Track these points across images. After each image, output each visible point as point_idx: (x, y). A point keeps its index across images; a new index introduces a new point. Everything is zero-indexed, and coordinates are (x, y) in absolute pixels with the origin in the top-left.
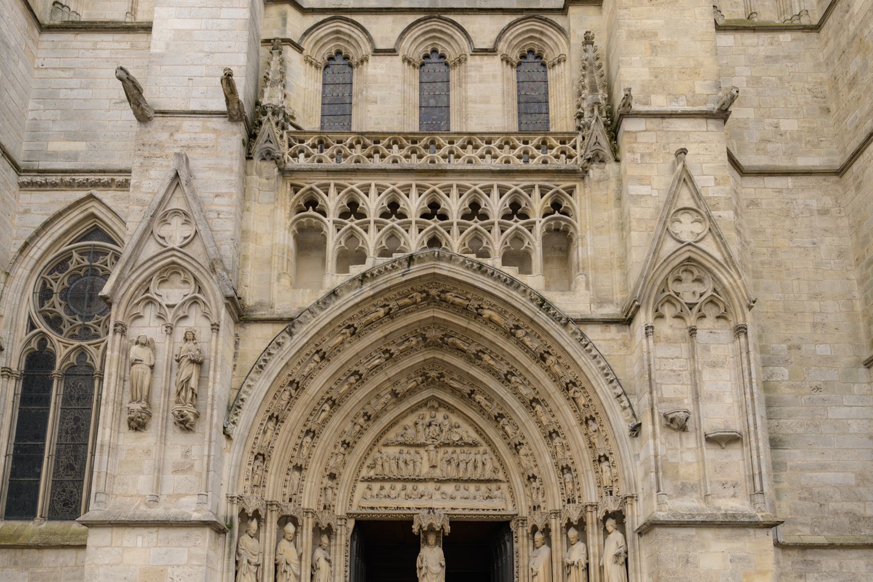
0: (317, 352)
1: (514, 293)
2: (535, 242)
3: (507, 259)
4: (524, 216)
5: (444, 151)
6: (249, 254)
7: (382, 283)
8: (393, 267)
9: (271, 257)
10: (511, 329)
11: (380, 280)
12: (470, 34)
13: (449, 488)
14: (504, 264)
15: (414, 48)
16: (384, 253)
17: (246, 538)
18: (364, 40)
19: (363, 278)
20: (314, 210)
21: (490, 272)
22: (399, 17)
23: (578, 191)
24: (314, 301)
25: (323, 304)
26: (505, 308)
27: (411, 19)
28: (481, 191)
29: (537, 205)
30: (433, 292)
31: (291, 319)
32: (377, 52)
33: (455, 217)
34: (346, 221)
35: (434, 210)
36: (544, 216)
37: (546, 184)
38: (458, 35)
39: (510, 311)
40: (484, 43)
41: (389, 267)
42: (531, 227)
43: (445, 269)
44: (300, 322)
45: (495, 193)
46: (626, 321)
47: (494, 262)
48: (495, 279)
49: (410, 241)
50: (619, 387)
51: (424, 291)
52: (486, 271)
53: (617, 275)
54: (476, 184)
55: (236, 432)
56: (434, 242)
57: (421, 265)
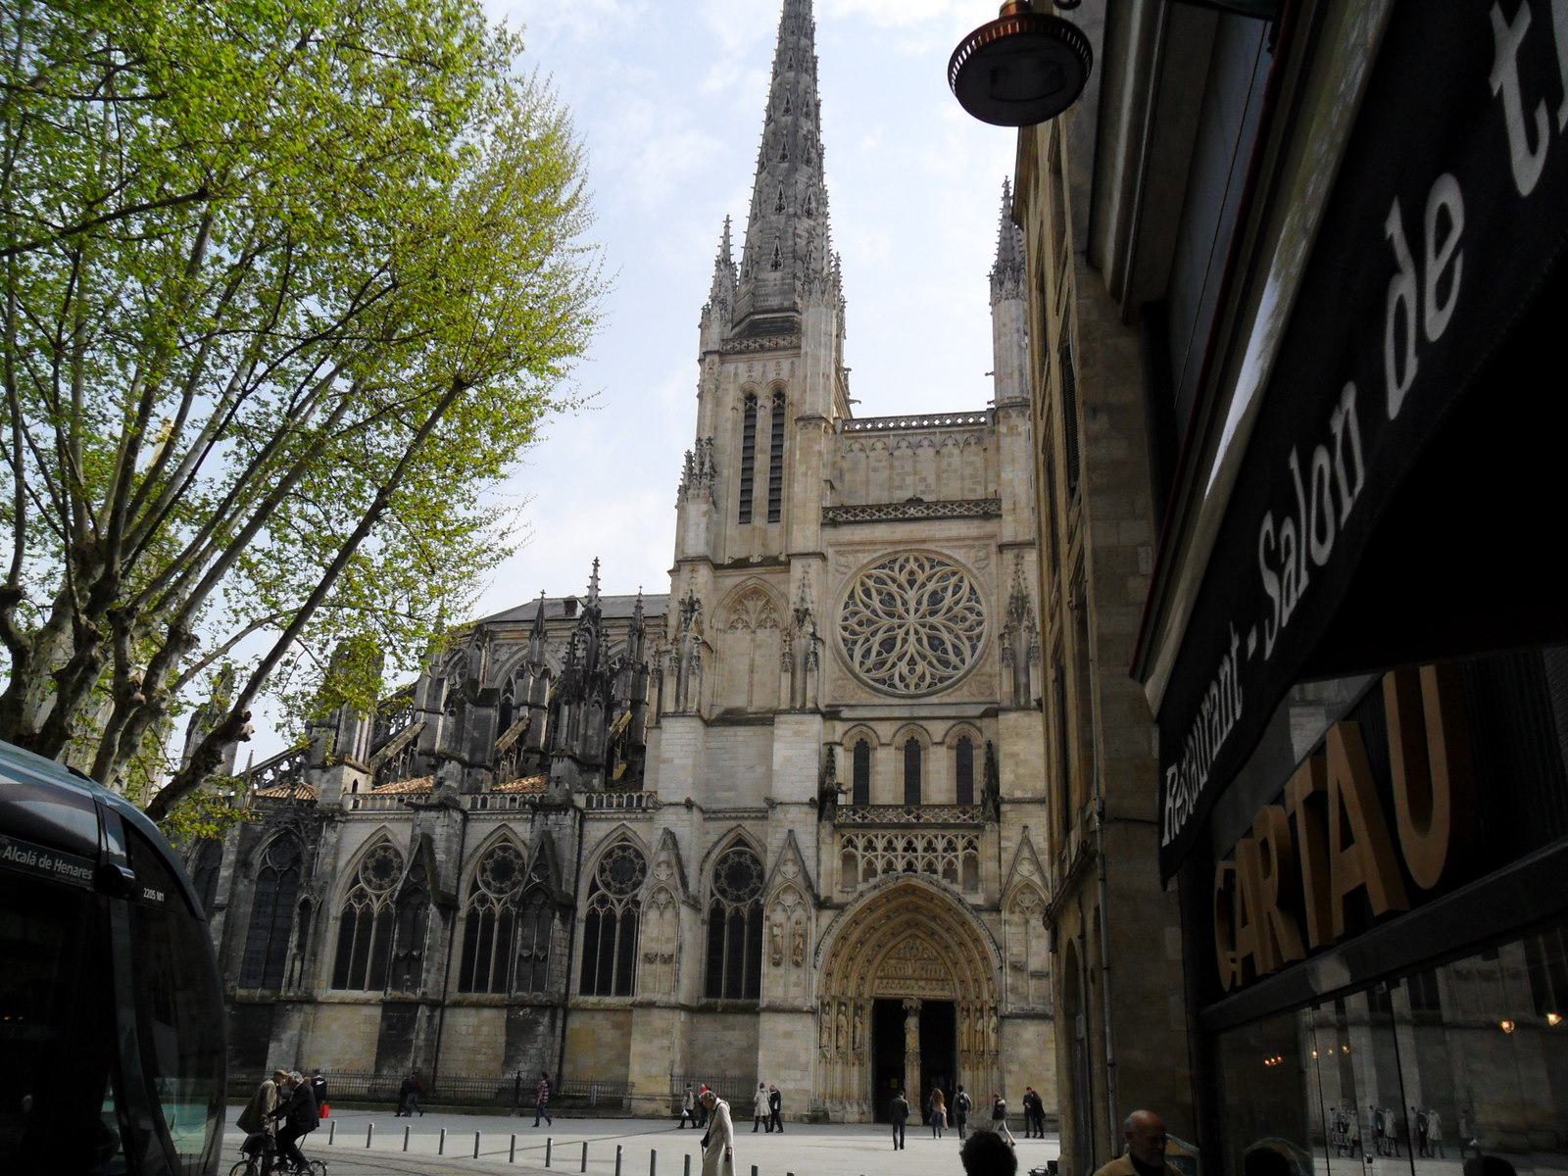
2: (959, 866)
3: (946, 874)
7: (884, 889)
13: (922, 983)
15: (901, 740)
16: (885, 871)
17: (824, 1015)
19: (875, 887)
25: (856, 900)
27: (899, 724)
29: (960, 844)
32: (883, 745)
33: (920, 848)
35: (910, 847)
42: (956, 857)
43: (914, 881)
45: (940, 838)
47: (938, 877)
54: (930, 833)
55: (818, 965)
56: (910, 867)
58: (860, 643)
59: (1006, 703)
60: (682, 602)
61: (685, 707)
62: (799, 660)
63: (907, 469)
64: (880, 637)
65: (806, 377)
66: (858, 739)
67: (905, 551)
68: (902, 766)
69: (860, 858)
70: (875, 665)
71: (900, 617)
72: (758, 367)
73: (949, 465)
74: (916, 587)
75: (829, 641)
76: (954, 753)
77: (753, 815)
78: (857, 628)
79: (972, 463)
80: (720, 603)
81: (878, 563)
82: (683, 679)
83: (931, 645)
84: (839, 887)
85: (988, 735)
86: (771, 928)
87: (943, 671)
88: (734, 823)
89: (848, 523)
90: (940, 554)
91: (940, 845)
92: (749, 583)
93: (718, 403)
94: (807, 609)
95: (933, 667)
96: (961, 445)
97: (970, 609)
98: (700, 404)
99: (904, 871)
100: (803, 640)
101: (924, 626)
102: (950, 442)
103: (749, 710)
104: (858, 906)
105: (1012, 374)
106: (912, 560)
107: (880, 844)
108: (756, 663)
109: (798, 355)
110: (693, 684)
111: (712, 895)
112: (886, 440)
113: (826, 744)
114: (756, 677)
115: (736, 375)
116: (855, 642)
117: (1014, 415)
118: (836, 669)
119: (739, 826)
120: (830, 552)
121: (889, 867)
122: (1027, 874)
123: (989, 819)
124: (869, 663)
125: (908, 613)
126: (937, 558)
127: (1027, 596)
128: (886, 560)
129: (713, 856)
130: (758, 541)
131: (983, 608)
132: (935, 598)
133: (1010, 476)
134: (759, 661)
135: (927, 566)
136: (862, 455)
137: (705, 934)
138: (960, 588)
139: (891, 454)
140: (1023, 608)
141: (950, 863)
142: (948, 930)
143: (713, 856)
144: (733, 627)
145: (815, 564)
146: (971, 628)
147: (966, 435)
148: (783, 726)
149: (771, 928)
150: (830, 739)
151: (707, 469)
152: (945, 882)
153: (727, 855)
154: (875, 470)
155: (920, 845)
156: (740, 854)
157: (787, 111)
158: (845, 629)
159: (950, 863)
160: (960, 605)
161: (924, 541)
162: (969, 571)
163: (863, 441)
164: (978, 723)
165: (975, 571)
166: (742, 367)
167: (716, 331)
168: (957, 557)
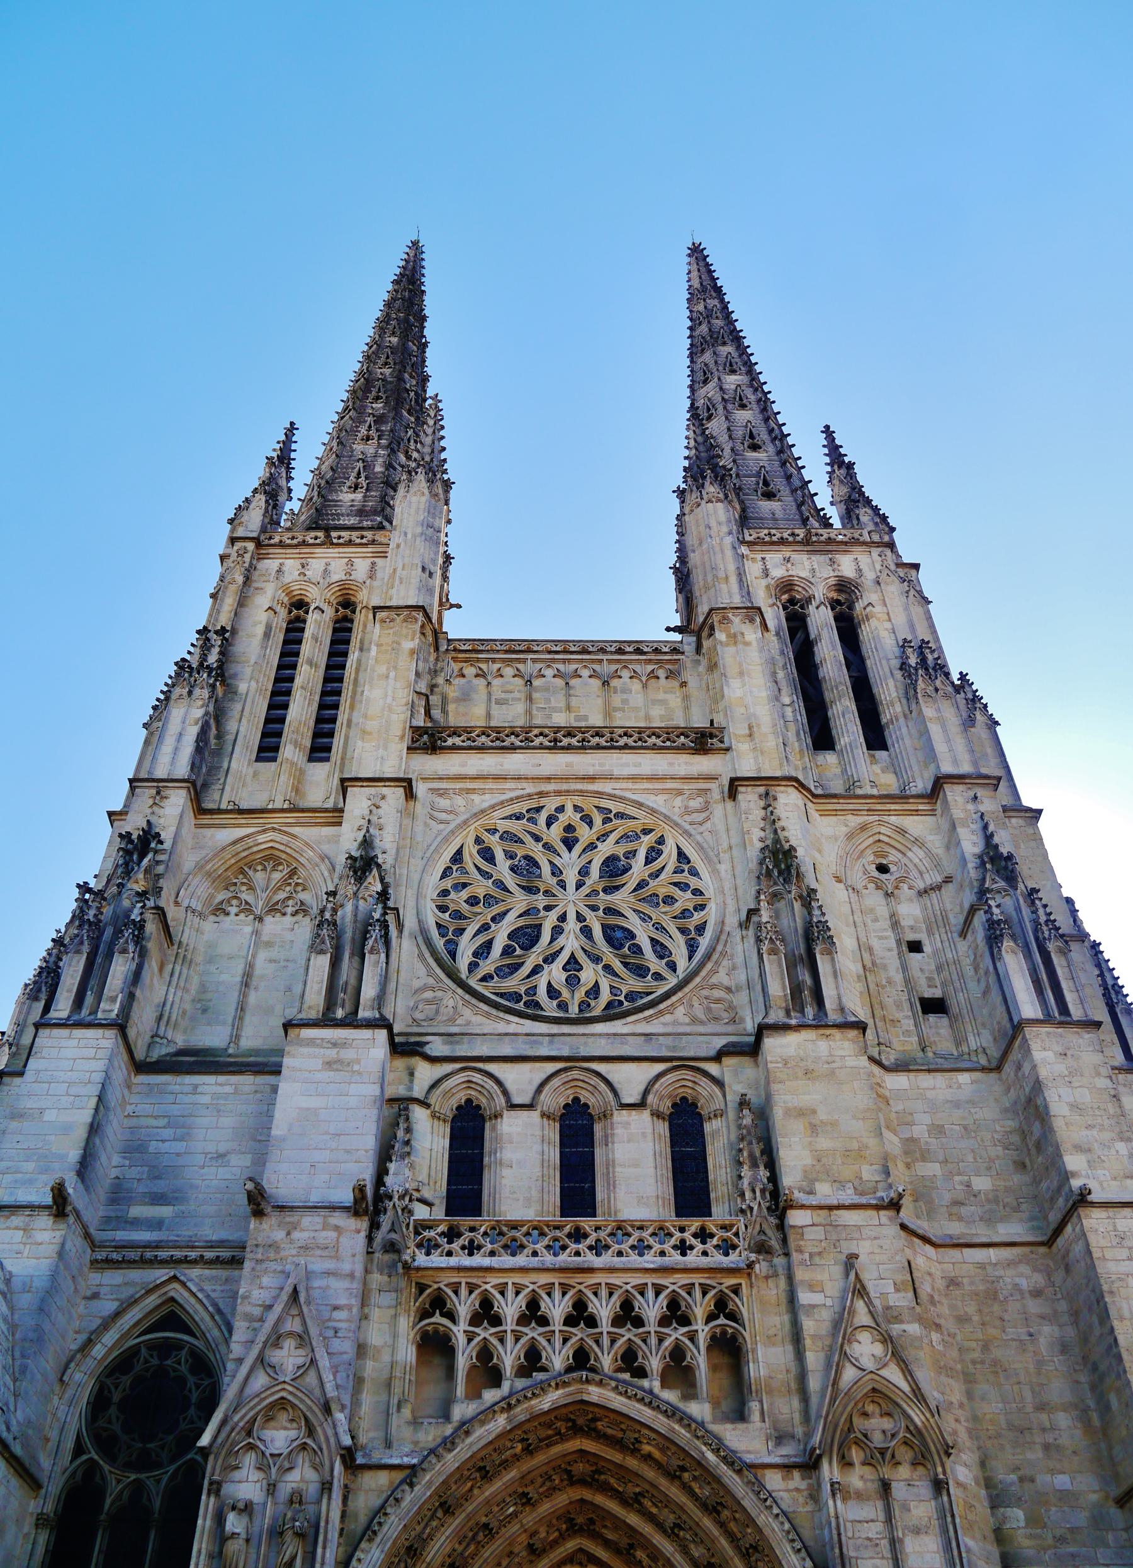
0: (442, 1505)
1: (677, 1427)
2: (700, 1360)
4: (685, 1321)
5: (590, 1241)
6: (366, 1375)
7: (521, 1413)
8: (533, 1394)
9: (391, 1378)
10: (675, 1471)
11: (518, 1409)
12: (616, 1085)
14: (664, 1385)
15: (555, 1098)
18: (499, 1092)
20: (442, 1315)
21: (647, 1400)
22: (538, 1065)
23: (745, 1290)
24: (439, 1440)
25: (449, 1443)
26: (667, 1444)
28: (632, 1291)
29: (700, 1308)
30: (581, 1421)
31: (414, 1466)
32: (513, 1107)
34: (477, 1330)
35: (580, 1315)
36: (707, 1323)
37: (708, 1282)
38: (602, 1086)
39: (674, 1449)
40: (631, 1095)
41: (529, 1395)
43: (594, 1394)
44: (424, 1470)
46: (810, 1465)
48: (653, 1409)
49: (553, 1357)
50: (808, 1559)
51: (570, 1420)
52: (643, 1399)
53: (796, 1403)
56: (581, 1359)
57: (567, 1390)
58: (471, 930)
59: (776, 1016)
60: (126, 837)
61: (94, 1012)
62: (348, 935)
63: (553, 704)
64: (510, 922)
65: (395, 570)
66: (461, 1097)
67: (558, 793)
68: (554, 1155)
69: (460, 1340)
70: (498, 970)
71: (547, 893)
72: (316, 567)
73: (625, 702)
74: (578, 849)
75: (410, 922)
76: (663, 1128)
77: (209, 1255)
78: (465, 908)
79: (663, 702)
80: (199, 867)
81: (508, 811)
82: (99, 960)
83: (609, 939)
84: (407, 1412)
85: (736, 1087)
86: (220, 1519)
87: (632, 983)
88: (161, 1274)
89: (454, 748)
90: (622, 799)
91: (652, 1309)
92: (261, 838)
93: (242, 602)
94: (376, 856)
95: (617, 975)
96: (644, 679)
97: (683, 886)
98: (214, 604)
99: (569, 1370)
100: (361, 902)
101: (594, 908)
102: (625, 674)
103: (231, 1051)
104: (452, 1460)
105: (727, 577)
106: (569, 808)
107: (510, 1309)
108: (258, 971)
109: (384, 555)
110: (120, 969)
111: (79, 1450)
112: (521, 666)
113: (391, 1101)
114: (253, 998)
115: (279, 571)
116: (460, 931)
117: (736, 620)
118: (422, 971)
119: (175, 1278)
120: (420, 789)
121: (532, 1360)
122: (869, 1364)
123: (762, 1248)
124: (487, 966)
125: (564, 887)
126: (615, 807)
127: (792, 849)
128: (522, 807)
129: (98, 1351)
130: (285, 782)
131: (706, 882)
132: (614, 869)
133: (739, 693)
134: (262, 966)
135: (598, 819)
136: (481, 682)
137: (40, 1549)
138: (660, 853)
139: (529, 682)
140: (789, 867)
141: (677, 1354)
142: (672, 1532)
143: (98, 1351)
144: (220, 910)
145: (395, 794)
146: (685, 914)
147: (650, 668)
148: (305, 1050)
149: (220, 1519)
150: (402, 1091)
151: (213, 658)
152: (670, 1396)
153: (134, 1352)
154: (498, 702)
155: (604, 1310)
156: (166, 1348)
157: (386, 364)
158: (443, 909)
159: (677, 1354)
160: (663, 876)
161: (592, 779)
162: (677, 824)
163: (484, 666)
164: (712, 1068)
165: (687, 827)
166: (291, 566)
167: (254, 519)
168: (655, 806)
